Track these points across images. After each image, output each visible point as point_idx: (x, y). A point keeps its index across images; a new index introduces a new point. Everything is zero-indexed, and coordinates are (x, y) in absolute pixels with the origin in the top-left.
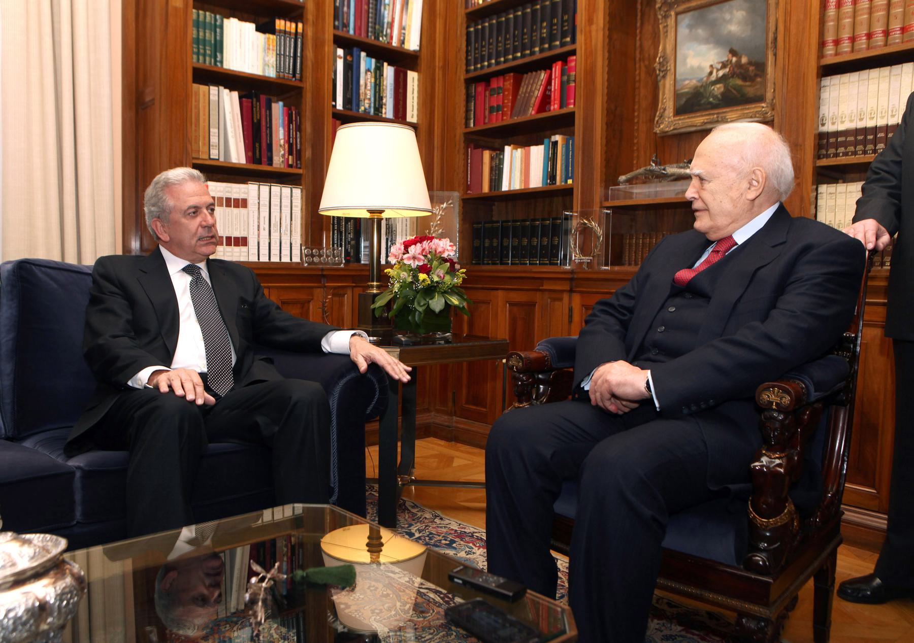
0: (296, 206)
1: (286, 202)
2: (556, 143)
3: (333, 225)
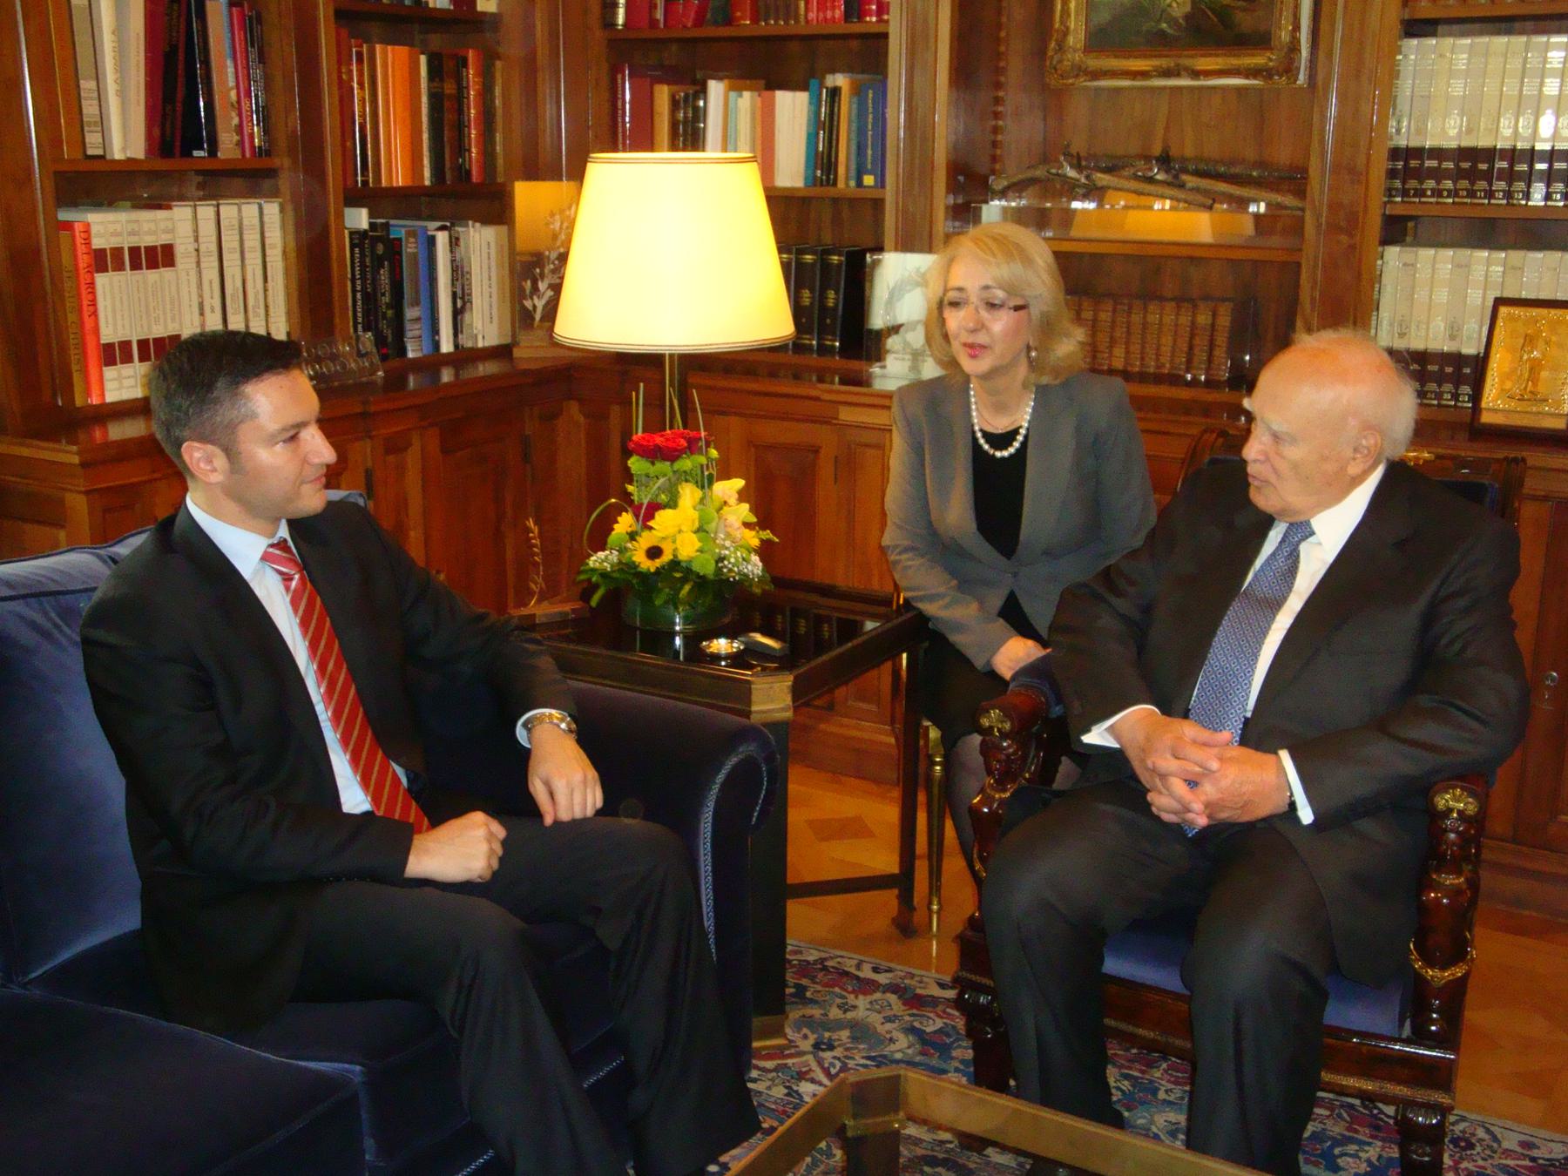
0: (273, 246)
1: (252, 240)
2: (835, 93)
3: (353, 280)
